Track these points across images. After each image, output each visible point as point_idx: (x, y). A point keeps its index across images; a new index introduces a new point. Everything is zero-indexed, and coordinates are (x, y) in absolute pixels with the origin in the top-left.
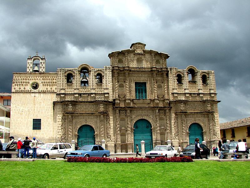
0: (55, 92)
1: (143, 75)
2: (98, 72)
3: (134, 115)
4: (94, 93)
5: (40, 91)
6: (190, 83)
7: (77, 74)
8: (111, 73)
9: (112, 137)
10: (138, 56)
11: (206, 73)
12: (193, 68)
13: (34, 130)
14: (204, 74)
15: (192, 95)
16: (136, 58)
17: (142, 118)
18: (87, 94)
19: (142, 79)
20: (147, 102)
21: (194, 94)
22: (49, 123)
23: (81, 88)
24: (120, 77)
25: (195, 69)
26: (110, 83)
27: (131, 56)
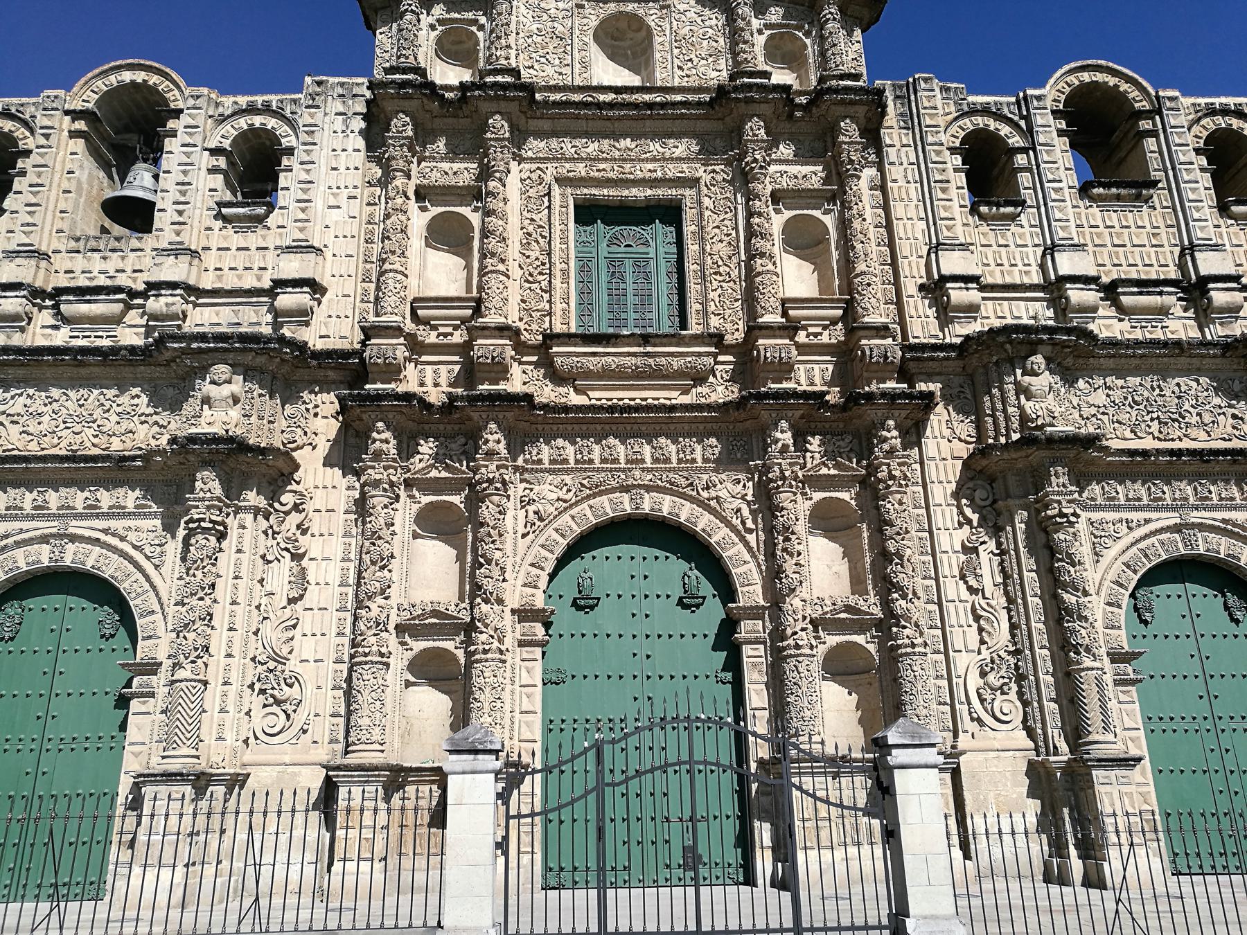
1: (655, 147)
2: (243, 123)
4: (173, 285)
7: (47, 136)
8: (358, 124)
9: (309, 689)
12: (1112, 81)
15: (1125, 300)
16: (594, 22)
17: (628, 508)
18: (119, 290)
20: (676, 363)
21: (1144, 285)
23: (72, 244)
25: (1124, 87)
26: (343, 200)
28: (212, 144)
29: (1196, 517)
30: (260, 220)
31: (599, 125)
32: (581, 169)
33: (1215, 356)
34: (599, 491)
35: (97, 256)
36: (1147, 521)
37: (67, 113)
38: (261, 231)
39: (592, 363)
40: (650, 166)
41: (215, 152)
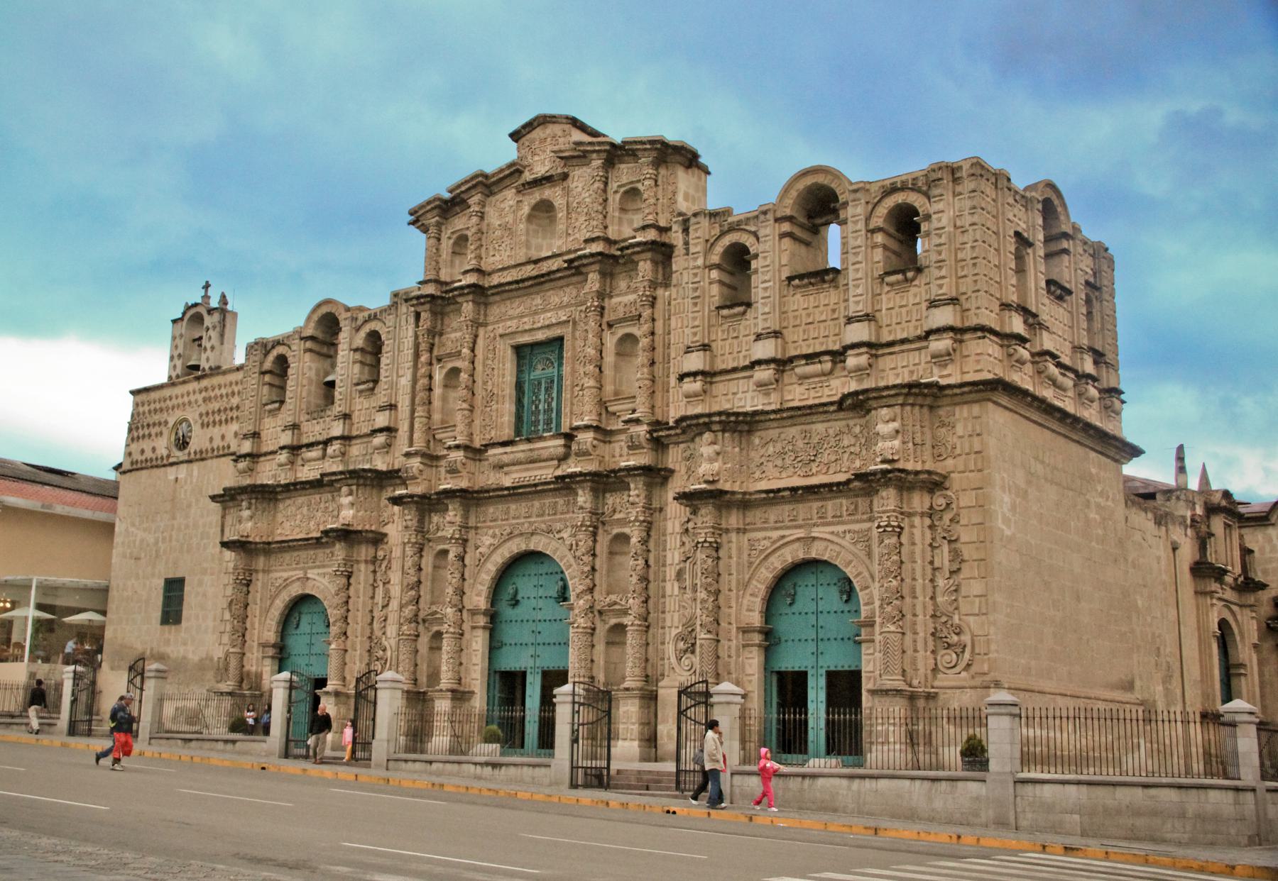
0: (232, 450)
3: (491, 532)
5: (192, 456)
6: (798, 287)
10: (537, 195)
11: (915, 189)
13: (166, 627)
14: (899, 198)
17: (523, 547)
19: (544, 319)
20: (545, 454)
21: (811, 358)
22: (205, 595)
24: (453, 336)
27: (506, 205)
28: (354, 346)
29: (816, 532)
30: (373, 389)
31: (519, 293)
32: (513, 325)
33: (834, 411)
34: (511, 536)
35: (315, 422)
36: (783, 537)
37: (302, 339)
38: (374, 397)
39: (506, 459)
40: (549, 315)
41: (356, 350)
